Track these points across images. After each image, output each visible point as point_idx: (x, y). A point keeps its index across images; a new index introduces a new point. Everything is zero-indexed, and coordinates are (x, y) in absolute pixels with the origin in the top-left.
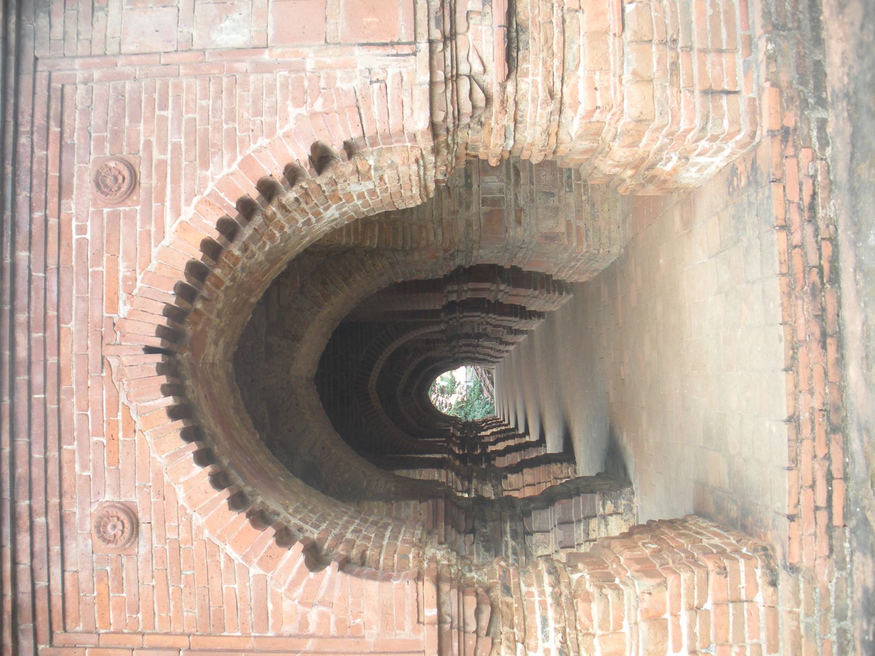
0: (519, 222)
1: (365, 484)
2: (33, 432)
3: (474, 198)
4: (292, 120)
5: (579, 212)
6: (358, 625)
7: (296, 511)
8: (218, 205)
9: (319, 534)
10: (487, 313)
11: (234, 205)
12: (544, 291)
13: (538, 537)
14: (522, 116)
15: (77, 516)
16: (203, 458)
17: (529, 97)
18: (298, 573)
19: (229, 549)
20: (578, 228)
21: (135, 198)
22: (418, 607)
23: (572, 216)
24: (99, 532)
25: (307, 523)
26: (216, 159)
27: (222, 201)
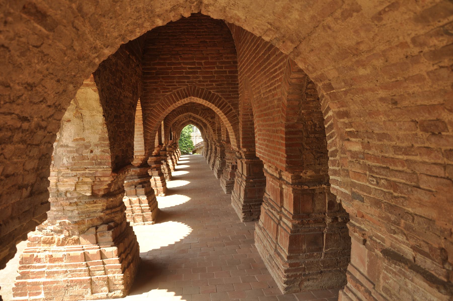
10: (246, 181)
12: (287, 267)
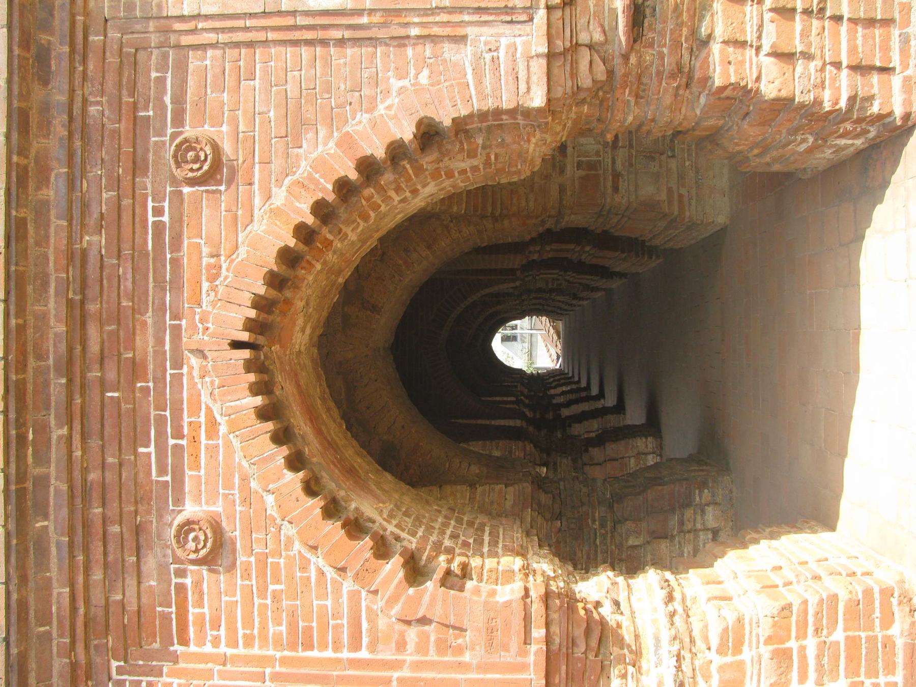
0: (616, 189)
1: (447, 466)
2: (106, 433)
3: (569, 161)
4: (394, 94)
5: (681, 177)
6: (460, 645)
7: (391, 516)
8: (313, 187)
9: (418, 543)
11: (330, 187)
13: (629, 525)
14: (644, 90)
15: (154, 524)
16: (295, 462)
17: (654, 70)
18: (397, 587)
19: (321, 562)
20: (681, 196)
21: (219, 177)
22: (525, 627)
23: (673, 184)
24: (178, 542)
25: (403, 530)
26: (310, 135)
27: (317, 183)
